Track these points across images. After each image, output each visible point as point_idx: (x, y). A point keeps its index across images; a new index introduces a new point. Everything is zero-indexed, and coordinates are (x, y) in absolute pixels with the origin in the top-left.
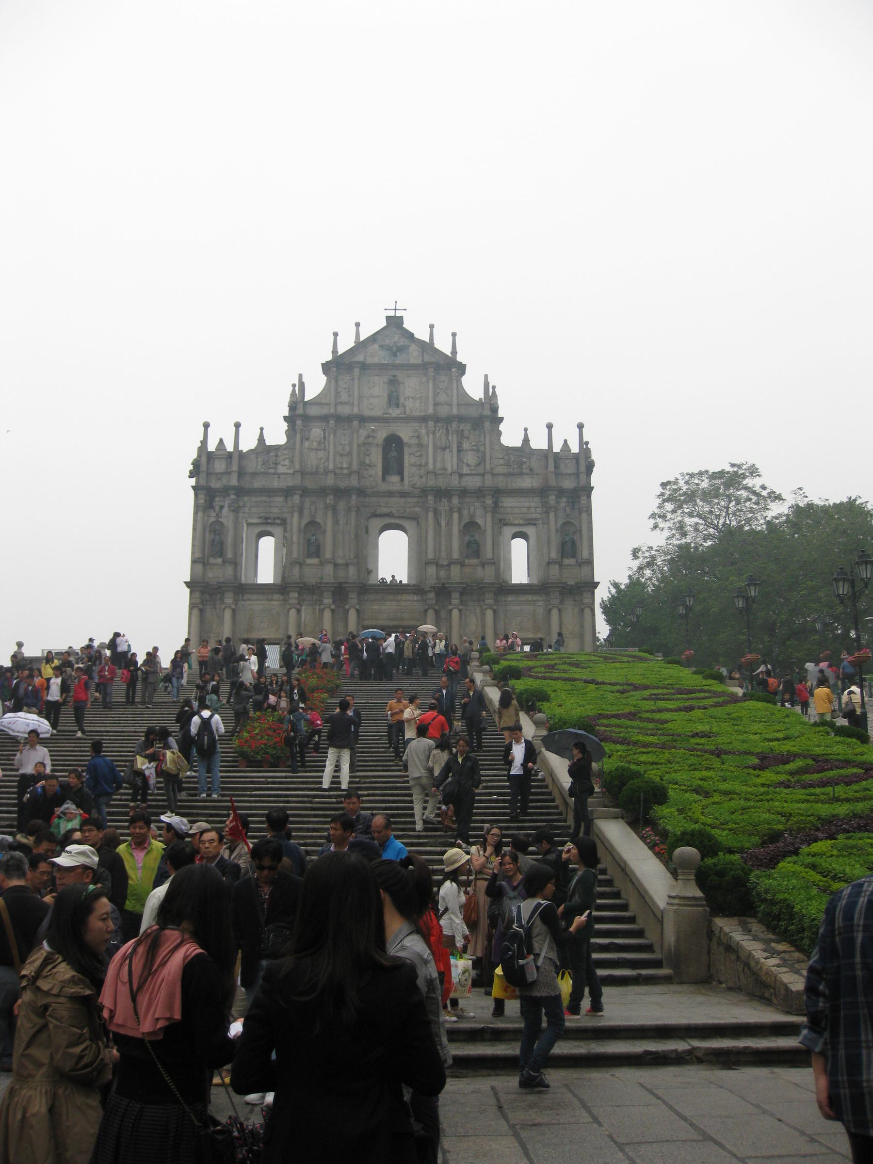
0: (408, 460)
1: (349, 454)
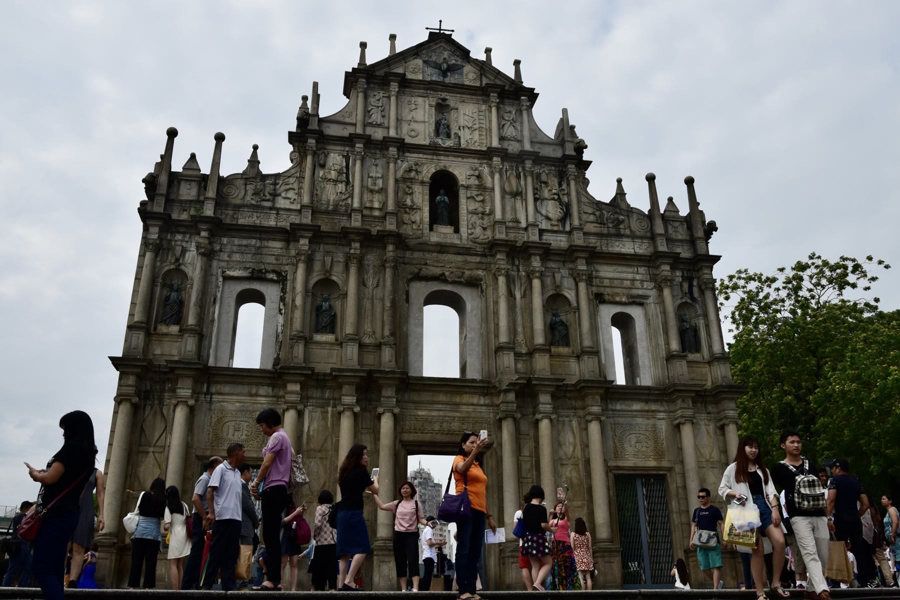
0: (465, 206)
1: (383, 191)
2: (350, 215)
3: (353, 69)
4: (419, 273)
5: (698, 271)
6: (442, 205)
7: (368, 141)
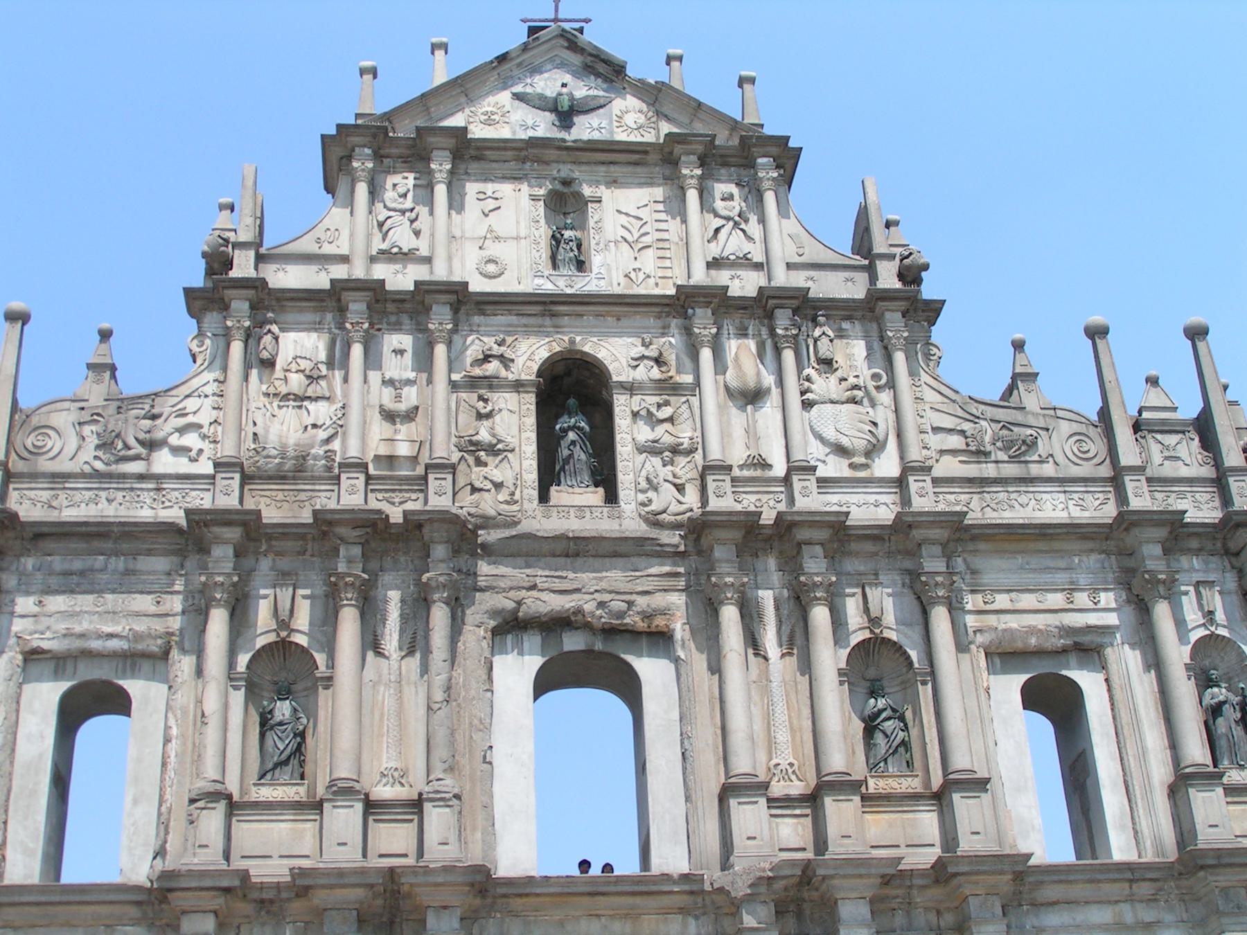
0: (628, 433)
2: (338, 478)
3: (339, 127)
4: (517, 610)
5: (1237, 554)
6: (572, 435)
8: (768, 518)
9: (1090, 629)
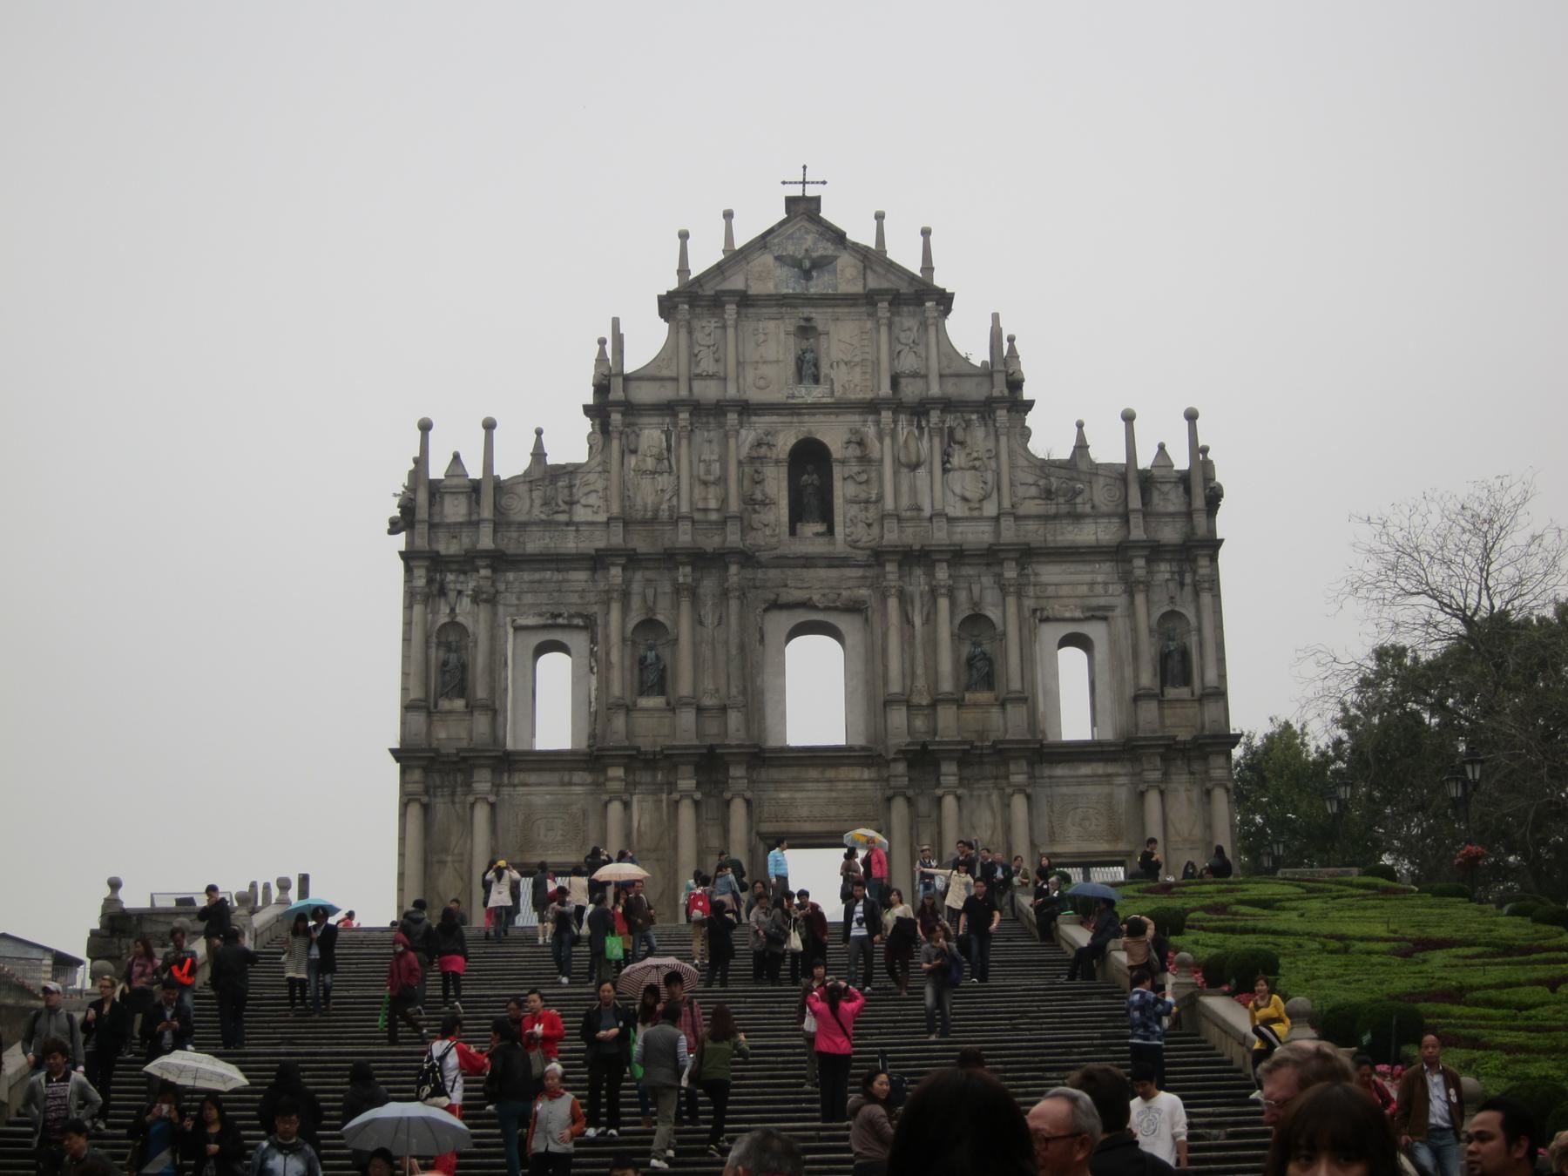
0: (841, 490)
1: (722, 480)
7: (698, 409)
8: (917, 547)
9: (1100, 608)
